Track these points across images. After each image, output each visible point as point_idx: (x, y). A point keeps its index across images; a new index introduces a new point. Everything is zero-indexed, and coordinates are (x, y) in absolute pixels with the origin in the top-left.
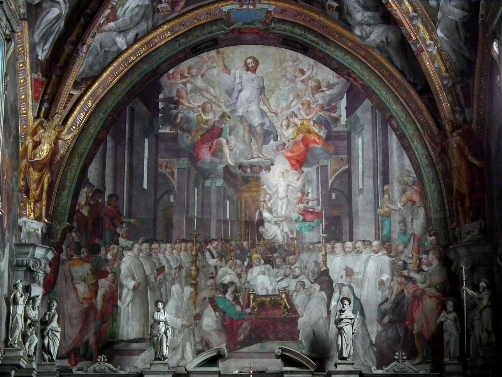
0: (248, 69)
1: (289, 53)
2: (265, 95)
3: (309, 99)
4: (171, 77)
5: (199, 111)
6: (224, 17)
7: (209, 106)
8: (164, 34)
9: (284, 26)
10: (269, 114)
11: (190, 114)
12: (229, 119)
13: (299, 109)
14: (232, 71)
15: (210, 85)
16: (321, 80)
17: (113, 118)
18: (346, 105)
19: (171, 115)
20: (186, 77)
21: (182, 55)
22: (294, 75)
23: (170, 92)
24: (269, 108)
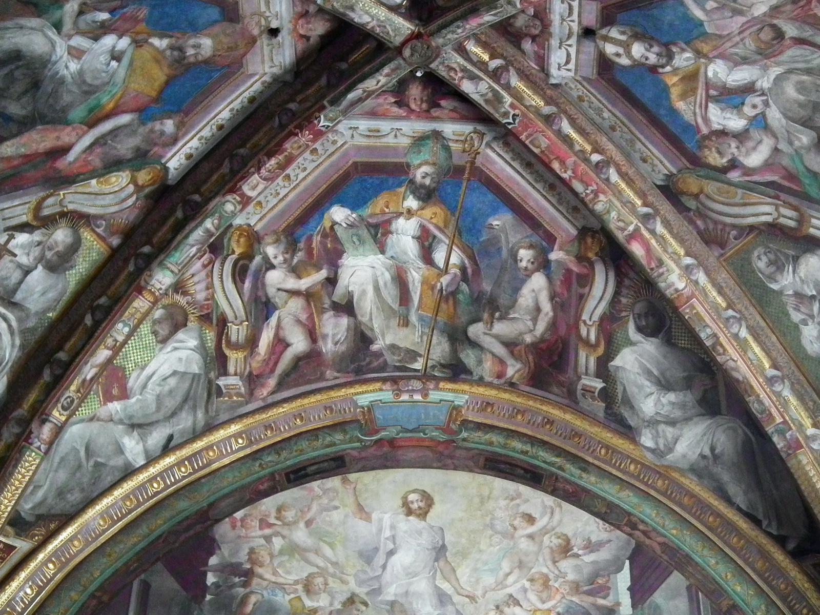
0: (409, 512)
1: (499, 485)
2: (447, 561)
3: (545, 570)
4: (239, 524)
5: (296, 591)
6: (361, 418)
7: (319, 581)
8: (228, 442)
9: (487, 436)
10: (456, 598)
11: (276, 595)
12: (364, 608)
13: (525, 591)
14: (374, 516)
15: (325, 542)
16: (570, 535)
17: (101, 602)
18: (629, 584)
19: (233, 598)
20: (270, 525)
21: (266, 485)
22: (512, 525)
23: (235, 552)
24: (457, 586)
